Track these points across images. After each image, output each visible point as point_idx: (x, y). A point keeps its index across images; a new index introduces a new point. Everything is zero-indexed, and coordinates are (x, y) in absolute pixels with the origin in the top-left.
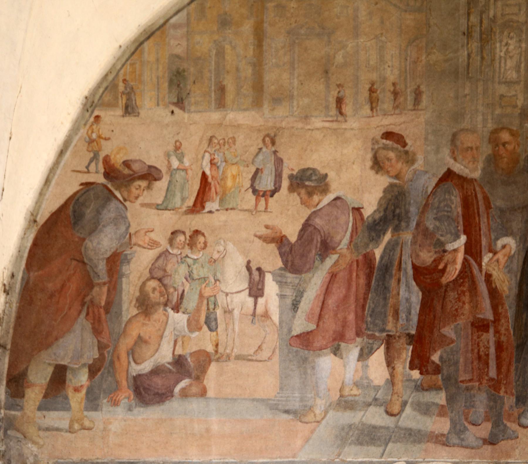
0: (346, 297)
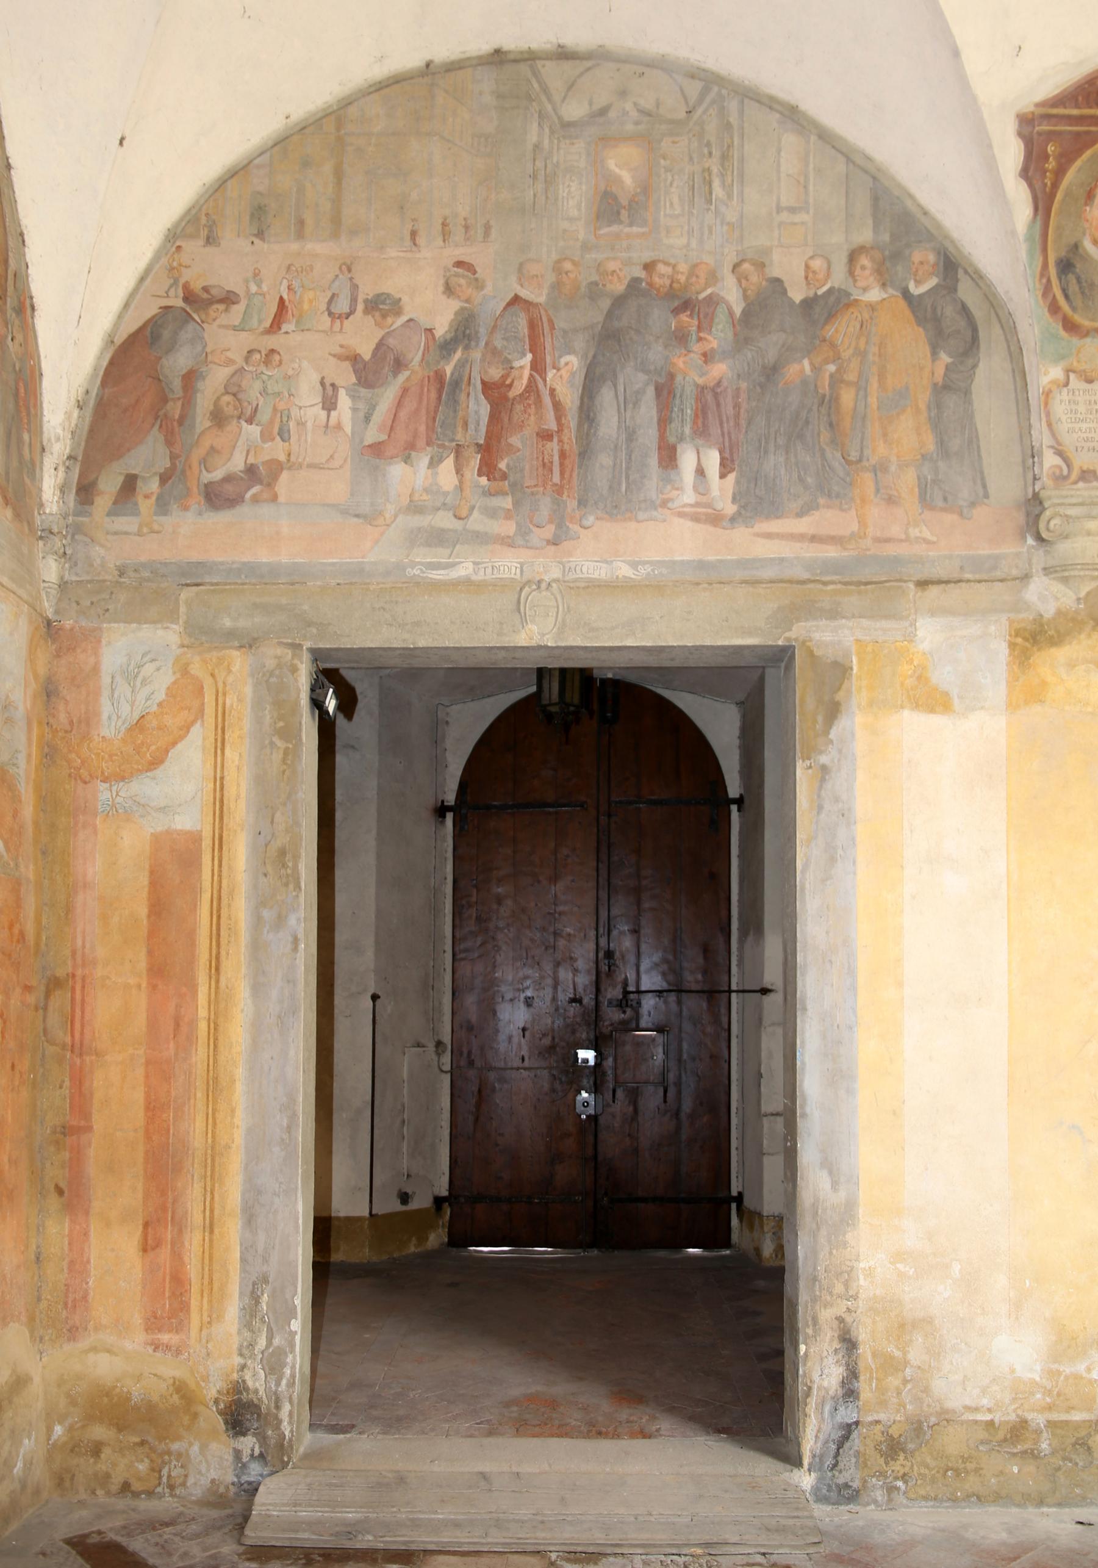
0: (417, 411)
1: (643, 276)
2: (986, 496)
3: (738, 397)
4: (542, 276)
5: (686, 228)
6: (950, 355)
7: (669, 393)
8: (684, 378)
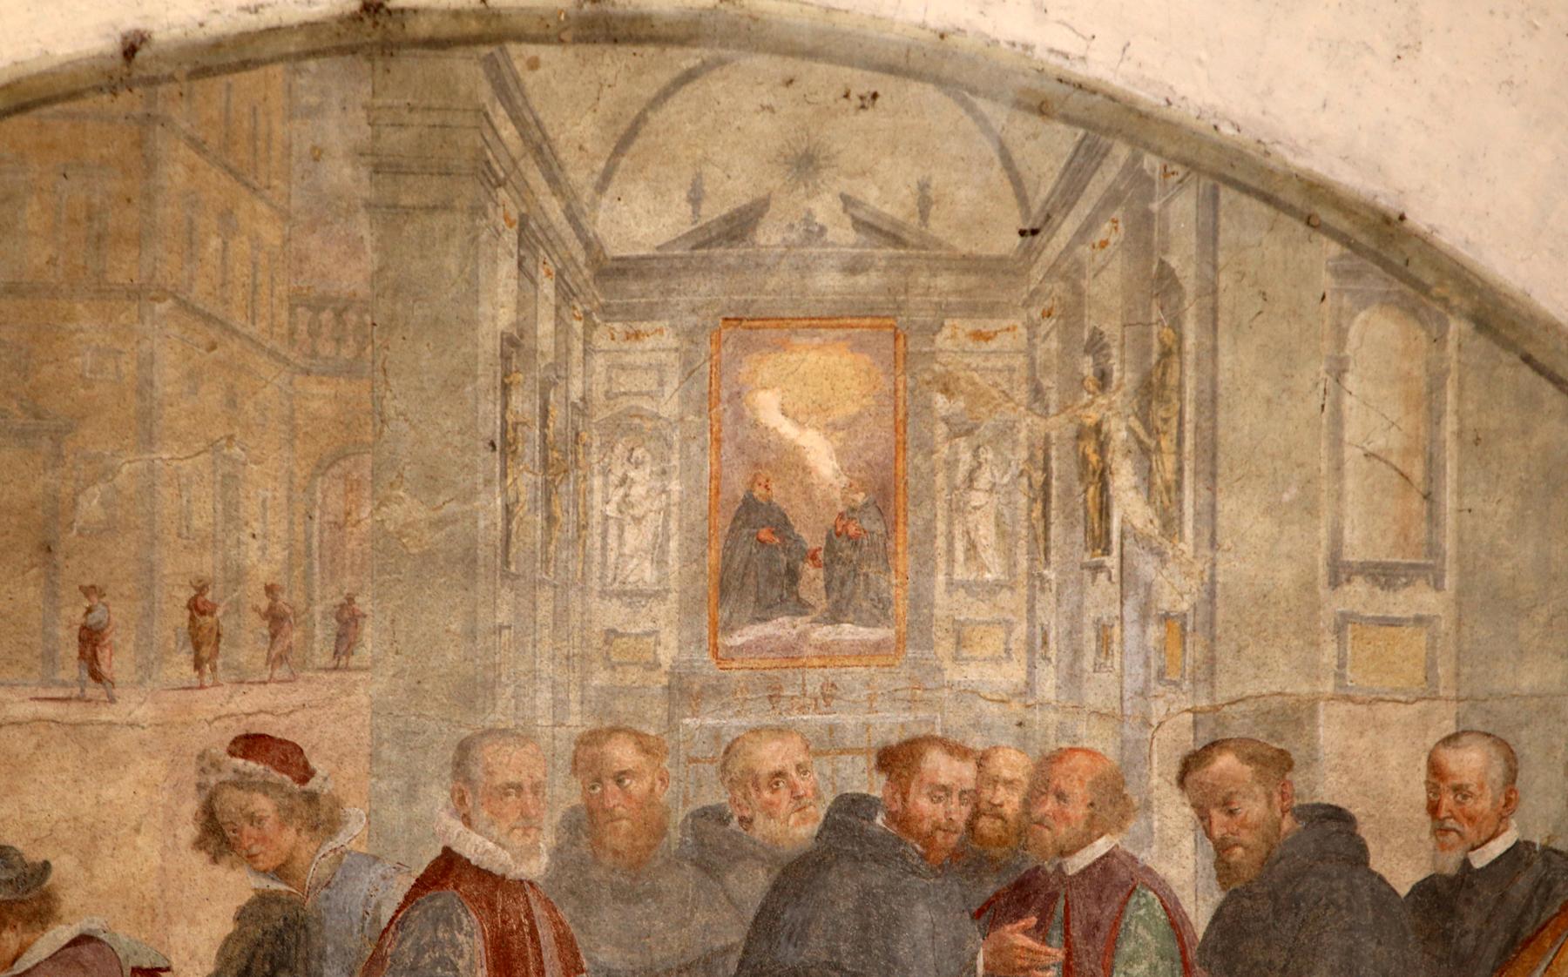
4: (536, 788)
5: (1021, 630)
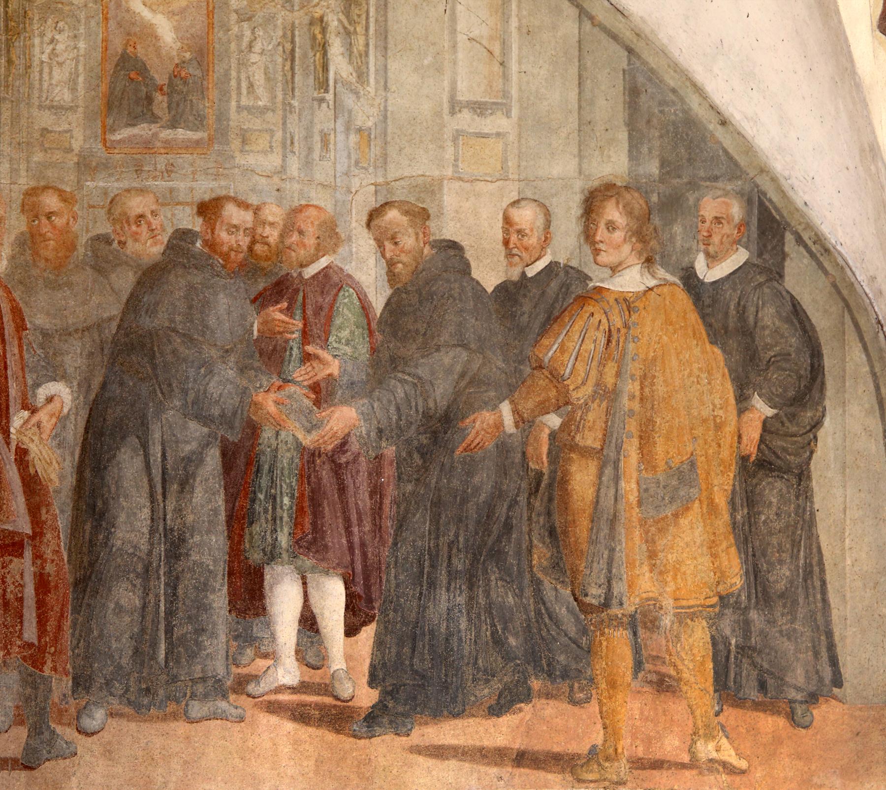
1: (197, 229)
2: (838, 681)
3: (379, 474)
5: (279, 135)
6: (771, 402)
7: (249, 464)
8: (277, 434)
